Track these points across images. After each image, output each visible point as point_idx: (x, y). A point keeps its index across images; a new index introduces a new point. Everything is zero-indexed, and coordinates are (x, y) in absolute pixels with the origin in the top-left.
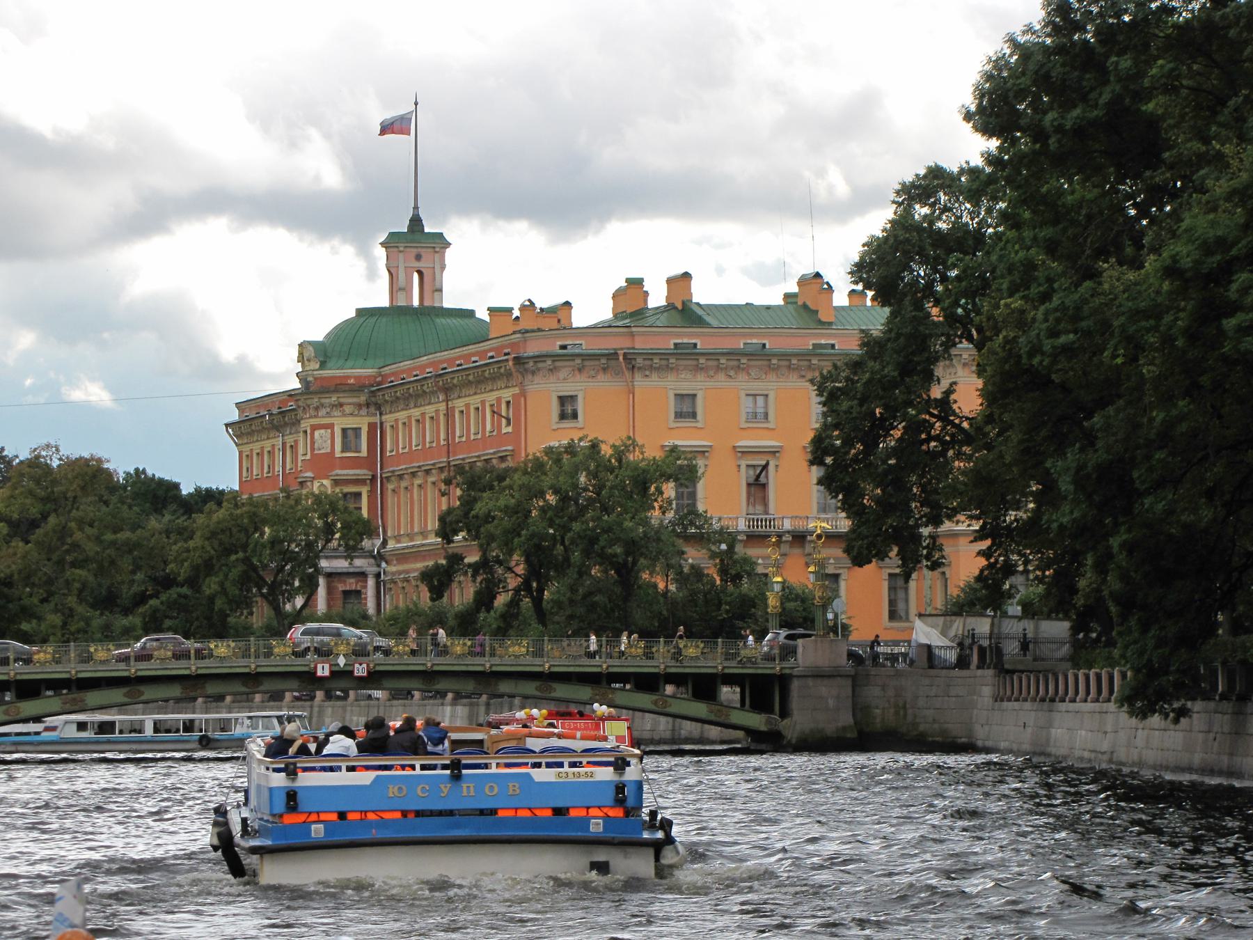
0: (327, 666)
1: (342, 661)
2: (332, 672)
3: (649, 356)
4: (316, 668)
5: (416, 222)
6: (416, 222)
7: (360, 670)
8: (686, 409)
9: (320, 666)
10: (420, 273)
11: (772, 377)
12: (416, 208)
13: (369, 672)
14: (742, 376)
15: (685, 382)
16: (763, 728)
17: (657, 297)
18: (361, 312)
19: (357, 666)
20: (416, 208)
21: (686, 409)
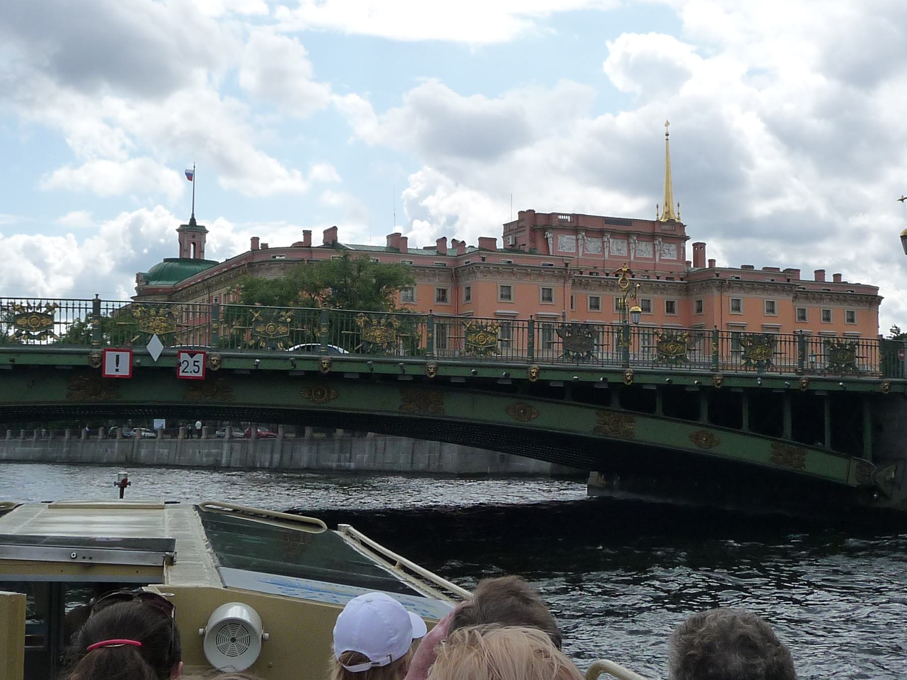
0: (125, 357)
1: (155, 348)
2: (134, 369)
4: (102, 358)
5: (193, 220)
6: (193, 220)
7: (191, 368)
9: (110, 357)
10: (194, 244)
12: (193, 214)
13: (207, 371)
16: (853, 482)
17: (317, 240)
18: (166, 260)
19: (184, 356)
20: (193, 214)
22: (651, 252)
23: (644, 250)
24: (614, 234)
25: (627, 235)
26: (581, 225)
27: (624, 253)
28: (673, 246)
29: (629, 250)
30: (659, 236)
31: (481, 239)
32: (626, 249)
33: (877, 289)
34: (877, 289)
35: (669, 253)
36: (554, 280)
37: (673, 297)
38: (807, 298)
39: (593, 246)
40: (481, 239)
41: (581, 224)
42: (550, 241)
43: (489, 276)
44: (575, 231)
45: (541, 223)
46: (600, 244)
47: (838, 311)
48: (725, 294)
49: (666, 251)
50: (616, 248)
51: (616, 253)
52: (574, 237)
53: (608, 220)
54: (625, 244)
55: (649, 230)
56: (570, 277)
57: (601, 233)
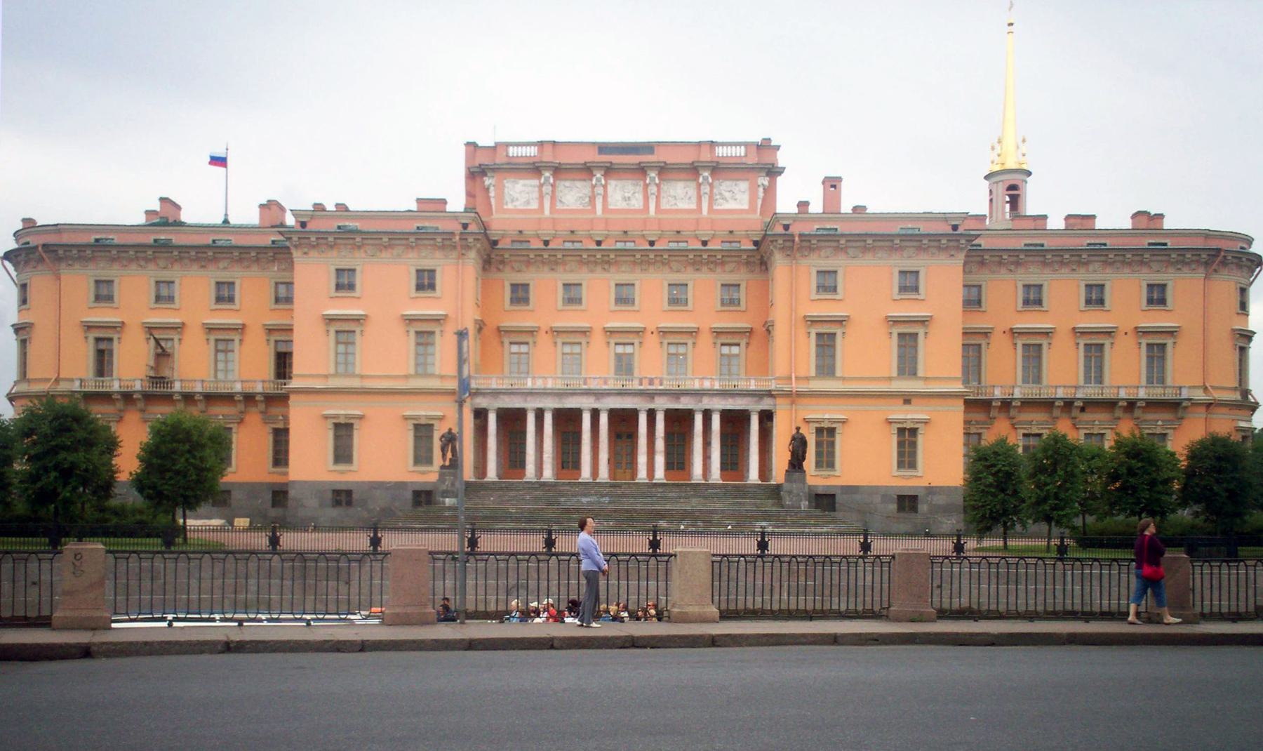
3: (68, 247)
8: (103, 293)
11: (177, 267)
14: (151, 266)
15: (105, 272)
21: (103, 293)
22: (694, 199)
23: (679, 197)
24: (610, 170)
25: (641, 170)
26: (554, 164)
27: (637, 203)
28: (744, 185)
29: (646, 198)
30: (705, 168)
31: (419, 201)
32: (640, 196)
33: (1249, 241)
34: (1249, 241)
35: (735, 198)
36: (438, 254)
37: (740, 276)
38: (1045, 264)
39: (572, 195)
40: (420, 201)
41: (548, 157)
42: (492, 194)
43: (314, 253)
44: (534, 169)
45: (482, 159)
46: (587, 191)
47: (1124, 291)
48: (804, 262)
49: (727, 195)
50: (623, 196)
51: (622, 205)
52: (536, 182)
53: (603, 148)
54: (640, 188)
55: (686, 158)
56: (468, 248)
57: (587, 170)
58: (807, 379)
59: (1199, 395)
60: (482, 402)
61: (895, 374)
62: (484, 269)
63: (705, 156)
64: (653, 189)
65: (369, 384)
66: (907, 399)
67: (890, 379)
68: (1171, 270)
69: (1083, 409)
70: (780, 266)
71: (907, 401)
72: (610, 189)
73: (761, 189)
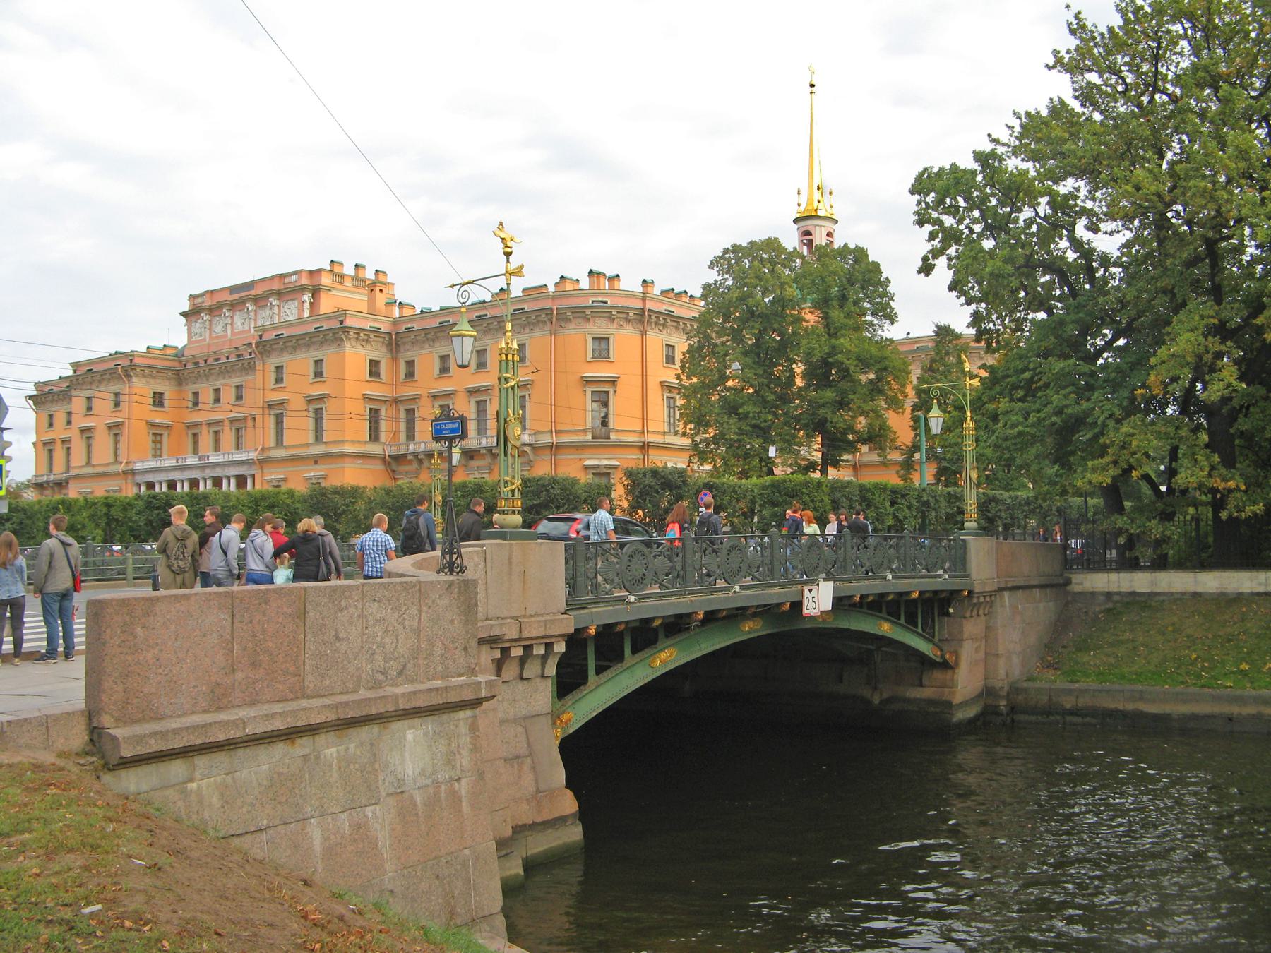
24: (233, 306)
48: (268, 361)
53: (233, 289)
58: (269, 449)
59: (546, 439)
60: (138, 478)
61: (311, 439)
62: (180, 384)
63: (276, 286)
64: (252, 314)
65: (97, 470)
66: (316, 460)
67: (307, 445)
68: (527, 330)
69: (472, 458)
70: (259, 366)
71: (316, 462)
72: (236, 318)
73: (307, 305)
